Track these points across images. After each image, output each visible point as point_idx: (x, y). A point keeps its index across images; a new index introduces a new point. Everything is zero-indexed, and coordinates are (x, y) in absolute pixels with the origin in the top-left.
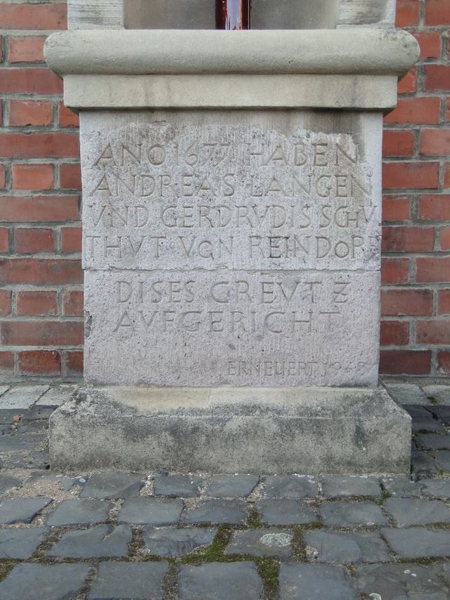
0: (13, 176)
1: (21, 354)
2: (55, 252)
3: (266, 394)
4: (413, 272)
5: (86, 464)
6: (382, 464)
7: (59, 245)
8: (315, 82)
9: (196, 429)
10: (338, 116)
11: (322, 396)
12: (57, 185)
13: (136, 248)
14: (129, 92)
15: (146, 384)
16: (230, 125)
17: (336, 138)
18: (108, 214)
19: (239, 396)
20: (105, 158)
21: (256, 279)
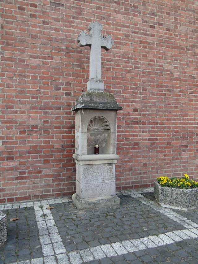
0: (55, 166)
1: (55, 194)
2: (61, 177)
3: (103, 198)
5: (83, 209)
6: (117, 205)
7: (61, 176)
8: (108, 161)
9: (96, 203)
10: (111, 164)
11: (110, 197)
12: (61, 167)
13: (88, 181)
14: (88, 163)
15: (89, 198)
16: (99, 166)
17: (110, 166)
19: (100, 198)
21: (102, 183)
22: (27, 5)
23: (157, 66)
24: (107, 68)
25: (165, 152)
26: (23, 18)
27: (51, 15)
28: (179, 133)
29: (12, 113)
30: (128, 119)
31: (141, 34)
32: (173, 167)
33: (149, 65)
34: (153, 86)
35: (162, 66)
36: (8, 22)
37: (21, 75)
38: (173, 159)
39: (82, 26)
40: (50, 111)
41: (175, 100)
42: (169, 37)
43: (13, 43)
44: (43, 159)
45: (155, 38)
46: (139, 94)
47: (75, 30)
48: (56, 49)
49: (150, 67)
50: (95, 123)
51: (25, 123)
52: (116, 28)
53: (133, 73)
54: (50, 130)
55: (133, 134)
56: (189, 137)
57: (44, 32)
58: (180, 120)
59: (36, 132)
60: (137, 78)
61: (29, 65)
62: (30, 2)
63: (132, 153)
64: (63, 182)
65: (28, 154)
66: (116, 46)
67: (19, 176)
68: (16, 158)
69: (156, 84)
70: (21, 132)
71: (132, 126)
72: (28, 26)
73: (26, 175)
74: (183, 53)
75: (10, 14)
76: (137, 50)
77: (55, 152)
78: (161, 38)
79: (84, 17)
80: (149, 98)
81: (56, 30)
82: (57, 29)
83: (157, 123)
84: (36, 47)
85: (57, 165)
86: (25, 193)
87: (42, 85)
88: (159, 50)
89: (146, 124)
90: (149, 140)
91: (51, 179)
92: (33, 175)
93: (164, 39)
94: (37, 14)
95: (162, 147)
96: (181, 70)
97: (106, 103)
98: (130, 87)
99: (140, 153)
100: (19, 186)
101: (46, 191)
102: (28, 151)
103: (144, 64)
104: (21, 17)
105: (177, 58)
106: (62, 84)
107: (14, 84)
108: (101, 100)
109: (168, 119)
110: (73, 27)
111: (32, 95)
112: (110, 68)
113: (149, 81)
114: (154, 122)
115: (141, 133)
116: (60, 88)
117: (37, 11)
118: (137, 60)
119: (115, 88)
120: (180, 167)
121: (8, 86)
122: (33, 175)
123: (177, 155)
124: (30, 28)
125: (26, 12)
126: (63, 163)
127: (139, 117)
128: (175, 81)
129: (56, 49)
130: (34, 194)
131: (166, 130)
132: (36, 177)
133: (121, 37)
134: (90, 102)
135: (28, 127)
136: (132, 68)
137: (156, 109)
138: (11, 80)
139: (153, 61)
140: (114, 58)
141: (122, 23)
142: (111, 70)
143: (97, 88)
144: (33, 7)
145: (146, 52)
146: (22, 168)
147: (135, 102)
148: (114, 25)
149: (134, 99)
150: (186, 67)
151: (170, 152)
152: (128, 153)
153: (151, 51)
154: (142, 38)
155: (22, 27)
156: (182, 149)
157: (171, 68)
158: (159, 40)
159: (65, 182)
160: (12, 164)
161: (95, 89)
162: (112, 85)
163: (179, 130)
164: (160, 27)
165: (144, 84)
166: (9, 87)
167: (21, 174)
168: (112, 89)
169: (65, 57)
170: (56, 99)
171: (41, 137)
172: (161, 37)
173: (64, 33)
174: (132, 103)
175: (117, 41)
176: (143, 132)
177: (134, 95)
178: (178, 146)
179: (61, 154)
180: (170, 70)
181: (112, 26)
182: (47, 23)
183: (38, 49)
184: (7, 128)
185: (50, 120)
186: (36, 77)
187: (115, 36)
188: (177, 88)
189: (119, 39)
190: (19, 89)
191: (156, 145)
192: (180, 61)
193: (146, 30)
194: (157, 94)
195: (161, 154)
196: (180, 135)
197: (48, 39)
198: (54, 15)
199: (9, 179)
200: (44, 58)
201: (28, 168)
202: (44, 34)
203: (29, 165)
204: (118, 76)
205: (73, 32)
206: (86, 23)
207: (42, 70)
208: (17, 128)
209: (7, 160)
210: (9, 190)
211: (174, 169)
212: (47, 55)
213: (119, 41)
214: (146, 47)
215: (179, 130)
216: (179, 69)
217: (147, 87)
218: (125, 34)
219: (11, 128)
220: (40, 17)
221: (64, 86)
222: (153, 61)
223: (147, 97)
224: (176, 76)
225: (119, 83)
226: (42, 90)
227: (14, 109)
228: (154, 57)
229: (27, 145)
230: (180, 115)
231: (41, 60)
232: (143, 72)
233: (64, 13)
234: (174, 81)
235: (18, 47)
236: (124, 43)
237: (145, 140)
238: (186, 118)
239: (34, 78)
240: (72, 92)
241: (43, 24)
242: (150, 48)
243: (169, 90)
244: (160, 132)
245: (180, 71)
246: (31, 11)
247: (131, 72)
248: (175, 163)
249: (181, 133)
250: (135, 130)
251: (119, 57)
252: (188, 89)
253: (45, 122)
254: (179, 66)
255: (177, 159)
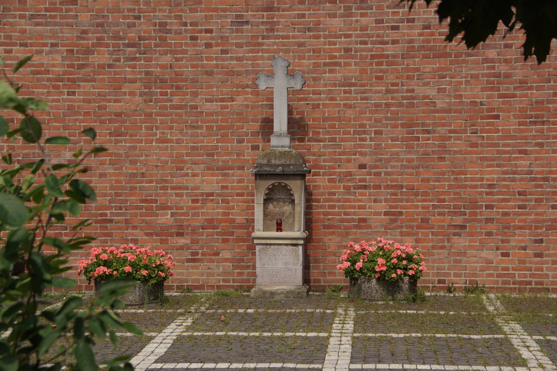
3: (285, 287)
4: (322, 267)
11: (292, 288)
18: (260, 259)
20: (260, 251)
22: (200, 32)
23: (403, 93)
24: (313, 105)
25: (417, 234)
26: (196, 51)
27: (232, 39)
28: (447, 203)
29: (182, 176)
30: (348, 181)
31: (373, 43)
32: (434, 261)
33: (388, 91)
34: (396, 126)
35: (413, 91)
36: (177, 59)
37: (193, 127)
38: (433, 247)
39: (275, 47)
40: (230, 172)
41: (439, 146)
42: (427, 40)
43: (184, 85)
44: (220, 237)
45: (400, 45)
46: (368, 140)
47: (266, 55)
48: (238, 86)
49: (390, 96)
50: (279, 191)
51: (197, 188)
52: (329, 42)
53: (357, 109)
54: (230, 198)
55: (357, 204)
56: (468, 211)
57: (222, 64)
58: (449, 180)
59: (212, 200)
60: (365, 115)
61: (202, 112)
62: (203, 28)
63: (355, 234)
64: (248, 271)
65: (202, 229)
66: (329, 70)
67: (190, 257)
68: (187, 234)
69: (400, 122)
70: (194, 201)
71: (356, 193)
72: (202, 61)
73: (200, 256)
74: (457, 62)
75: (180, 49)
76: (366, 70)
77: (236, 229)
78: (411, 43)
79: (278, 33)
80: (387, 146)
81: (239, 59)
82: (239, 57)
83: (401, 187)
84: (211, 87)
85: (239, 247)
86: (198, 281)
87: (220, 137)
88: (407, 65)
89: (381, 189)
90: (386, 214)
91: (231, 264)
92: (208, 257)
93: (416, 45)
94: (213, 42)
95: (412, 227)
96: (452, 94)
97: (289, 165)
98: (352, 131)
99: (370, 235)
100: (191, 270)
101: (224, 281)
102: (202, 226)
103: (379, 92)
104: (193, 50)
105: (444, 73)
106: (247, 134)
107: (185, 138)
108: (282, 162)
109: (423, 180)
110: (264, 51)
111: (207, 152)
112: (319, 104)
113: (387, 119)
114: (395, 186)
115: (372, 203)
116: (244, 139)
117: (212, 38)
118: (365, 86)
119: (326, 135)
120: (450, 262)
121: (178, 141)
122: (208, 257)
123: (442, 241)
124: (205, 62)
125: (199, 41)
126: (248, 244)
127: (368, 177)
128: (440, 115)
129: (238, 86)
130: (208, 283)
131: (420, 197)
132: (212, 261)
133: (338, 54)
134: (267, 165)
135: (202, 194)
136: (357, 100)
137: (400, 164)
138: (181, 133)
139: (393, 85)
140: (325, 89)
141: (340, 31)
142: (321, 107)
143: (281, 144)
144: (208, 33)
145: (381, 71)
146: (194, 248)
147: (361, 154)
148: (325, 37)
149: (359, 150)
150: (464, 86)
151: (429, 236)
152: (348, 234)
153: (392, 69)
154: (374, 50)
155: (194, 62)
156: (452, 231)
157: (432, 92)
158: (408, 47)
159: (250, 271)
160: (182, 241)
161: (278, 147)
162: (321, 130)
163: (447, 197)
164: (409, 26)
165: (378, 124)
166: (178, 143)
167: (194, 256)
168: (321, 136)
169: (250, 96)
170: (238, 155)
171: (218, 207)
172: (411, 41)
173: (250, 62)
174: (356, 155)
175: (330, 61)
176: (375, 201)
177: (359, 143)
178: (443, 226)
179: (245, 231)
180: (430, 95)
181: (322, 40)
182: (226, 52)
183: (215, 89)
184: (177, 195)
185: (230, 185)
186: (212, 127)
187: (328, 54)
188: (444, 125)
189: (335, 57)
190: (191, 144)
191: (399, 223)
192: (452, 78)
193: (381, 35)
194: (403, 140)
195: (409, 238)
196: (449, 207)
197: (227, 73)
198: (236, 39)
199: (178, 261)
200: (223, 100)
201: (202, 247)
202: (222, 68)
203: (203, 244)
204: (332, 116)
205: (262, 58)
206: (281, 42)
207: (220, 117)
208: (188, 195)
209: (176, 236)
210: (179, 274)
211: (435, 265)
212: (226, 96)
213: (333, 61)
214: (383, 62)
215: (447, 199)
216: (447, 93)
217: (384, 129)
218: (344, 48)
219: (181, 195)
220: (217, 45)
221: (250, 137)
222: (393, 85)
223: (383, 145)
224: (440, 104)
225: (333, 126)
226: (220, 144)
227: (185, 171)
228: (397, 78)
229: (200, 217)
230: (449, 172)
231: (218, 103)
232: (376, 105)
233: (249, 34)
234: (437, 115)
235: (189, 90)
236: (342, 63)
237: (379, 214)
238: (463, 176)
239: (209, 128)
240: (260, 145)
241: (221, 54)
242: (389, 64)
243: (426, 130)
244: (407, 201)
245: (450, 96)
246: (206, 39)
247: (355, 107)
248: (438, 254)
249: (452, 204)
250: (360, 197)
251: (334, 85)
252: (468, 125)
253: (223, 188)
254: (448, 87)
255: (443, 247)
